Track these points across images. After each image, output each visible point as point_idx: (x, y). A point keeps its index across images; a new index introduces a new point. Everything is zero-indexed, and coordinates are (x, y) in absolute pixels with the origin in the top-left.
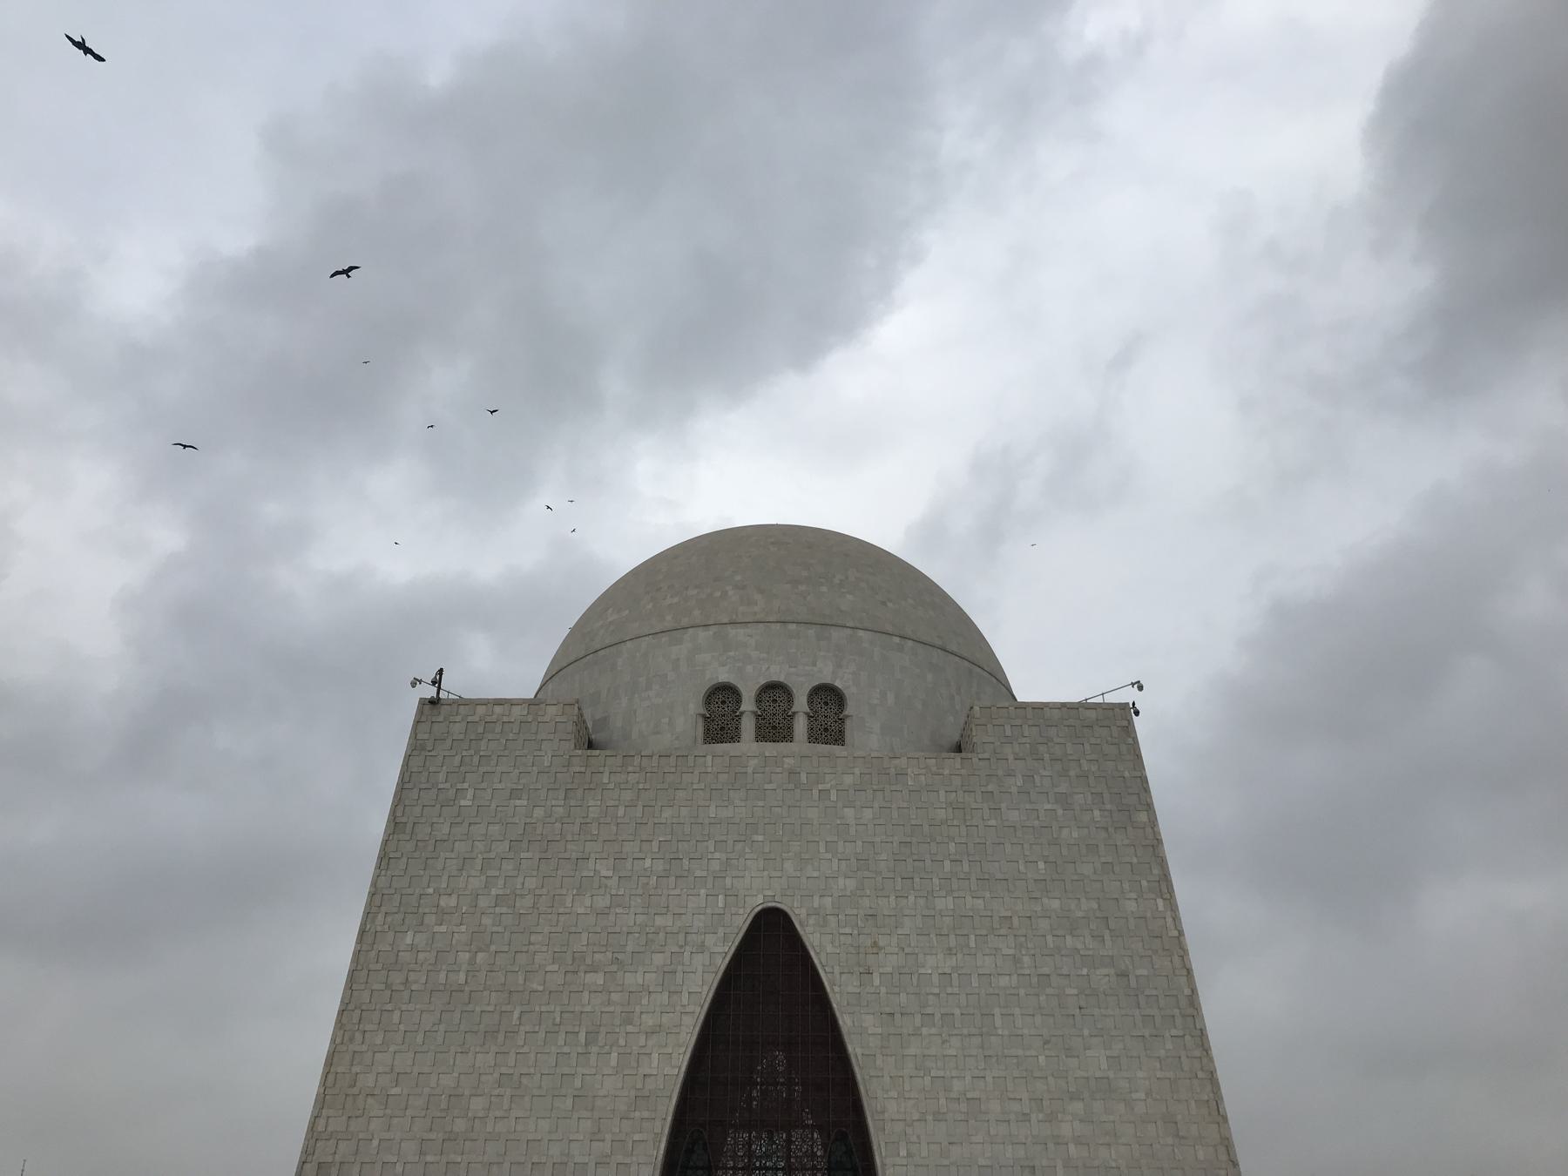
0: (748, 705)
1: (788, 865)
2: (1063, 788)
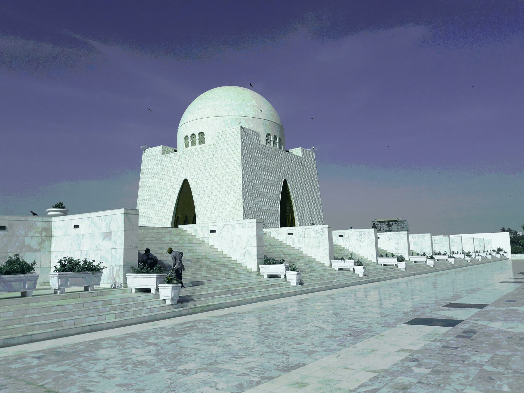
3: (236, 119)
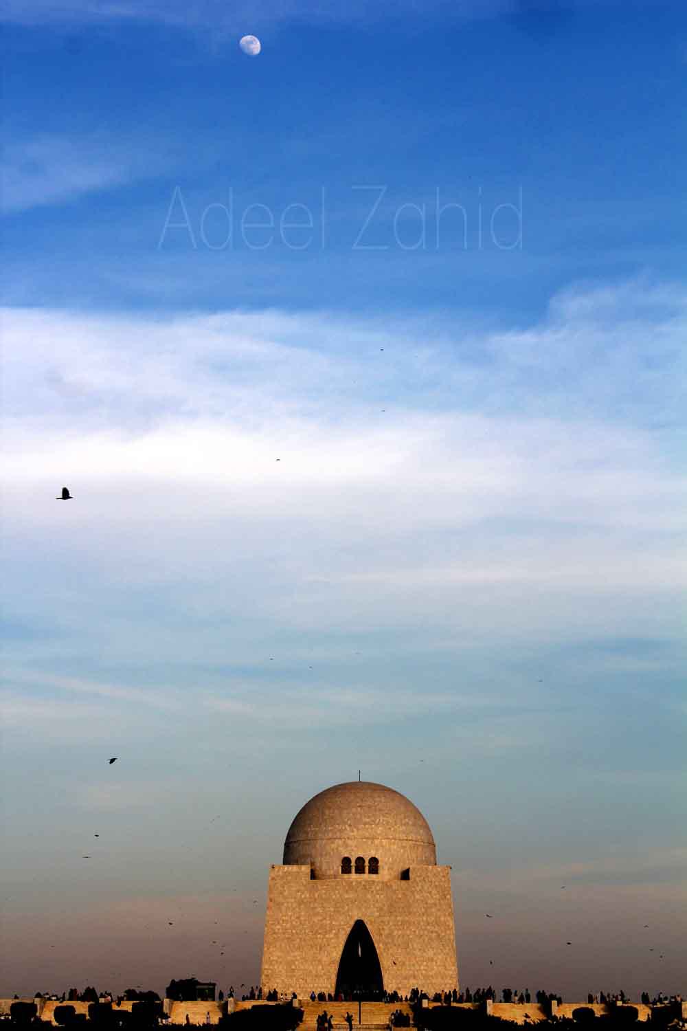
0: (353, 864)
1: (363, 910)
2: (430, 889)
3: (415, 844)
